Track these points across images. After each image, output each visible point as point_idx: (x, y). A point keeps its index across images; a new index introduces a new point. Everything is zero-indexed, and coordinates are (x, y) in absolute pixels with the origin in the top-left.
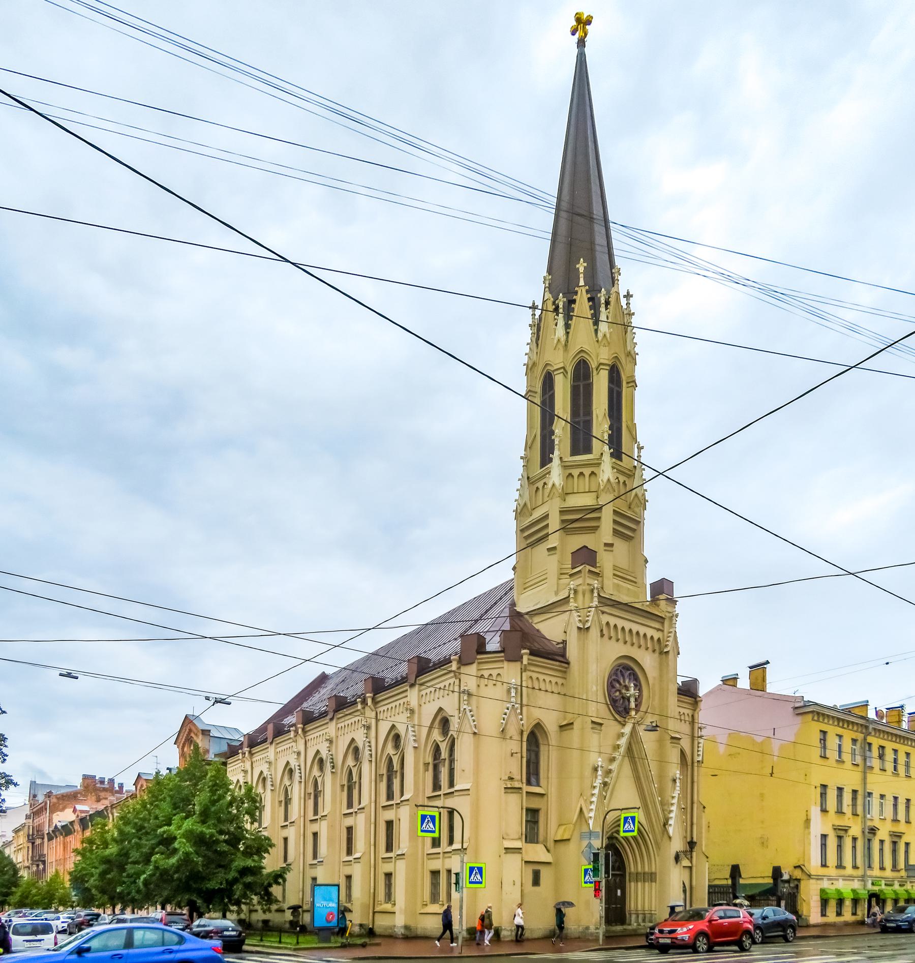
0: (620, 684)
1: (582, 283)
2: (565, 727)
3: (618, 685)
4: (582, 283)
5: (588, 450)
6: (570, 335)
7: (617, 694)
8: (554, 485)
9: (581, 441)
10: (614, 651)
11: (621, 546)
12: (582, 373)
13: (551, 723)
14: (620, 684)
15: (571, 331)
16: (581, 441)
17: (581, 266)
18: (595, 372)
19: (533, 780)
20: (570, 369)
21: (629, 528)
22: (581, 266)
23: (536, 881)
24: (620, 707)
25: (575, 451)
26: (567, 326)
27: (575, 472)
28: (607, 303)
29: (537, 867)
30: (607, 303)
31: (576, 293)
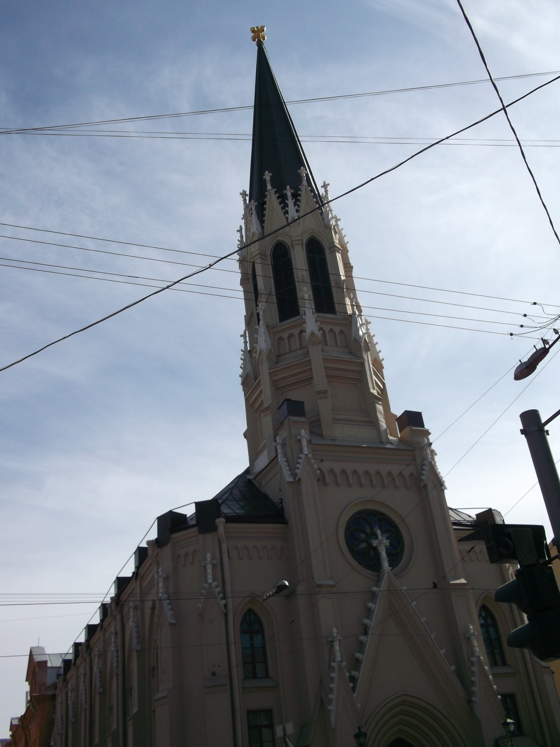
0: (366, 534)
1: (269, 187)
3: (363, 536)
4: (269, 187)
6: (265, 228)
7: (364, 545)
8: (260, 351)
14: (366, 534)
15: (265, 225)
17: (267, 176)
18: (291, 249)
20: (269, 252)
22: (267, 176)
24: (368, 560)
28: (296, 196)
30: (296, 196)
31: (266, 196)
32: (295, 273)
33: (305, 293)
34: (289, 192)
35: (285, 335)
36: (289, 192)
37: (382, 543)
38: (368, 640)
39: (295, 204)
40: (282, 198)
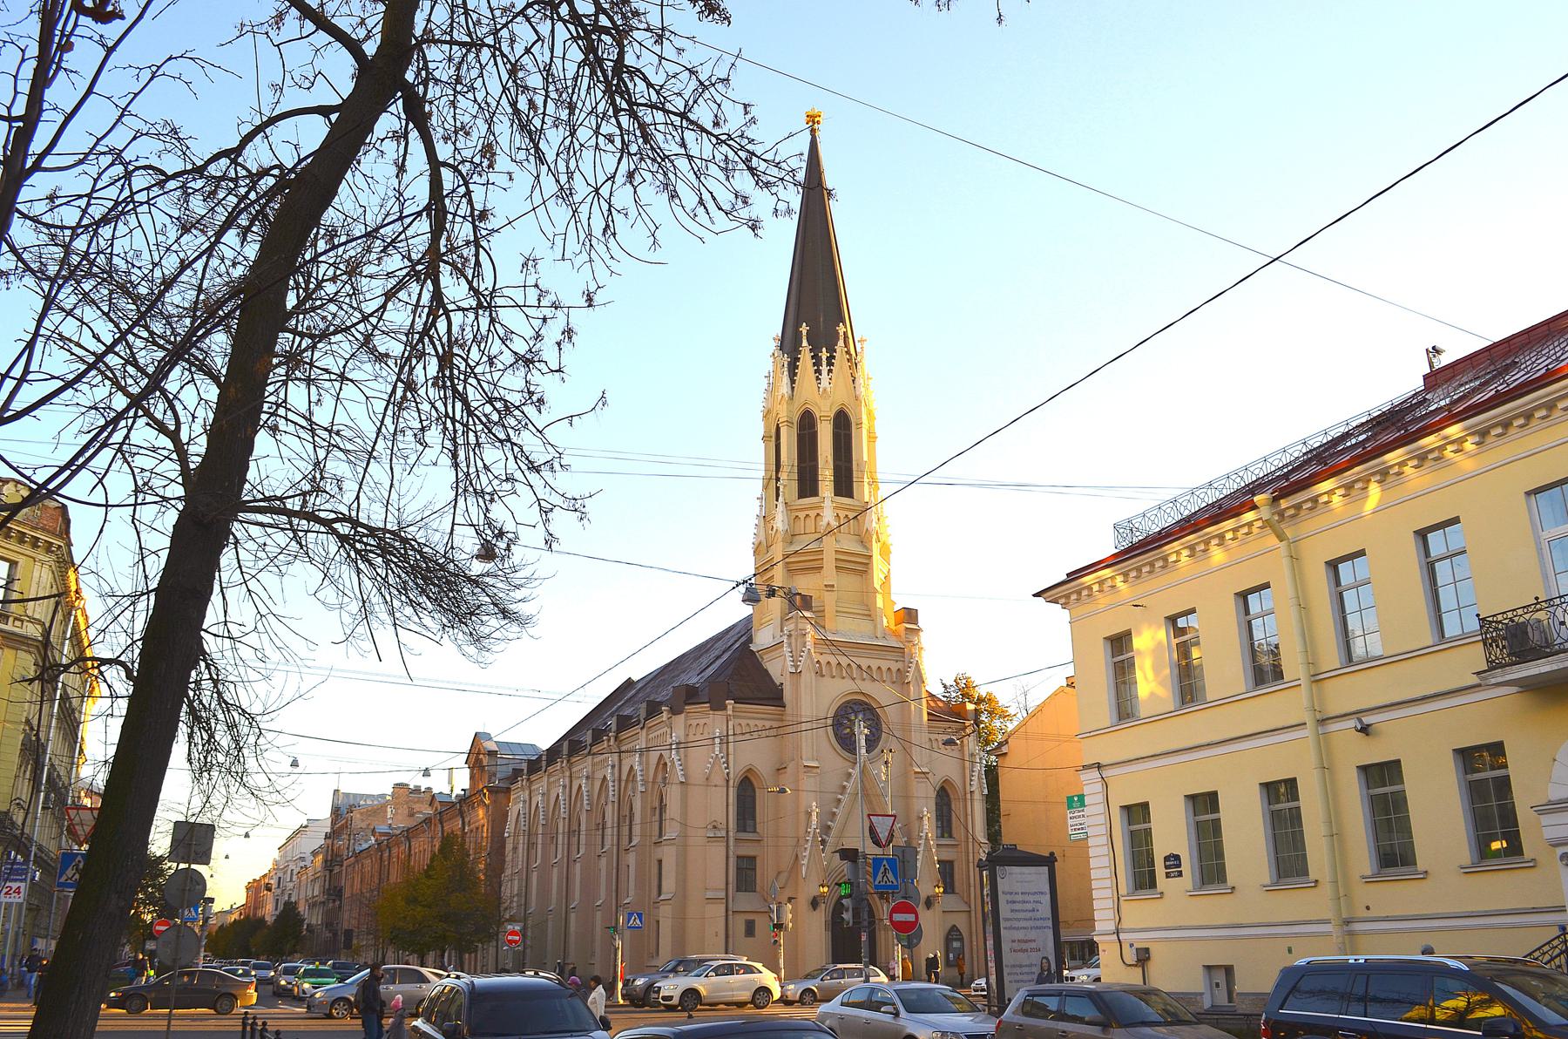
1: (805, 343)
2: (780, 770)
4: (805, 343)
5: (815, 493)
9: (808, 486)
10: (836, 691)
11: (849, 582)
12: (807, 424)
13: (764, 767)
16: (808, 486)
17: (804, 329)
19: (750, 822)
20: (796, 419)
21: (859, 566)
22: (804, 329)
23: (750, 929)
25: (800, 497)
26: (793, 382)
27: (802, 515)
29: (751, 917)
32: (818, 457)
33: (826, 473)
34: (824, 355)
35: (802, 515)
36: (824, 355)
37: (862, 732)
38: (845, 798)
39: (830, 371)
40: (817, 363)
